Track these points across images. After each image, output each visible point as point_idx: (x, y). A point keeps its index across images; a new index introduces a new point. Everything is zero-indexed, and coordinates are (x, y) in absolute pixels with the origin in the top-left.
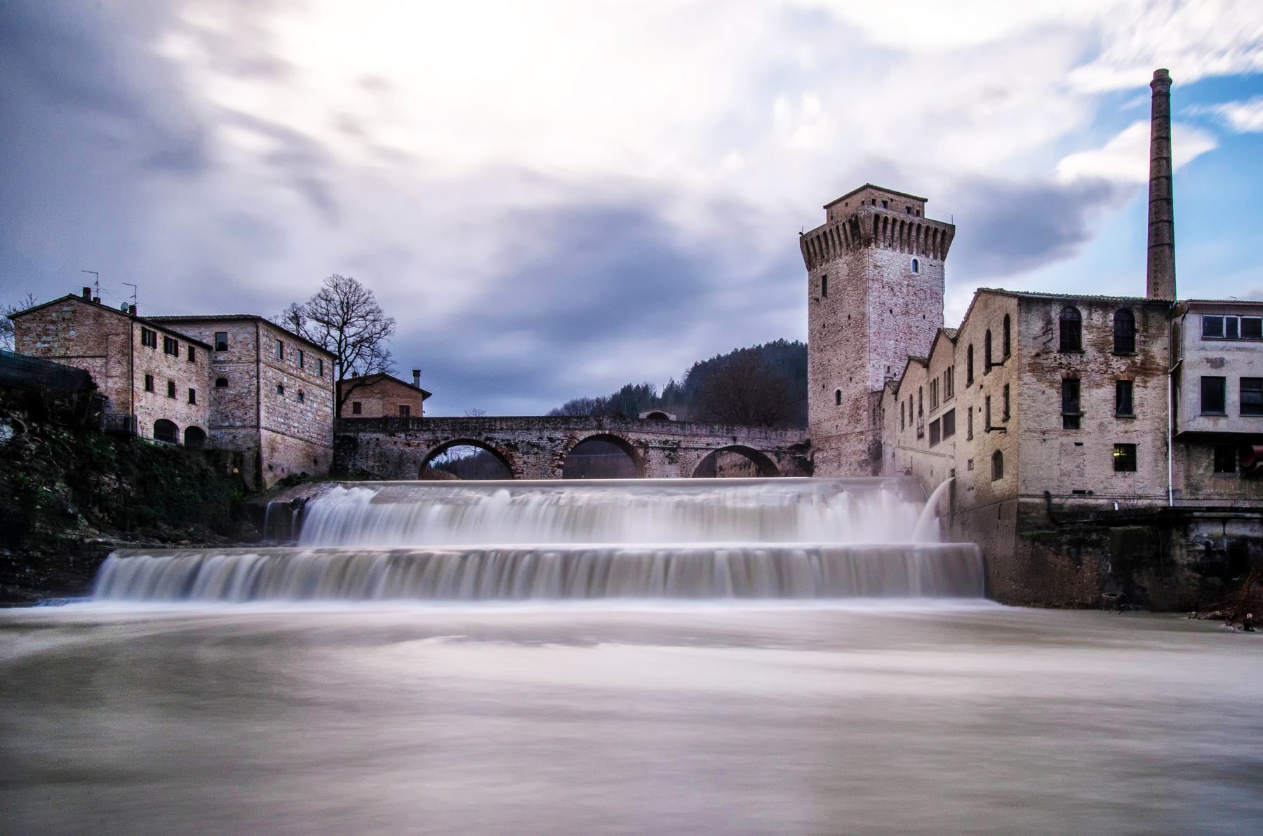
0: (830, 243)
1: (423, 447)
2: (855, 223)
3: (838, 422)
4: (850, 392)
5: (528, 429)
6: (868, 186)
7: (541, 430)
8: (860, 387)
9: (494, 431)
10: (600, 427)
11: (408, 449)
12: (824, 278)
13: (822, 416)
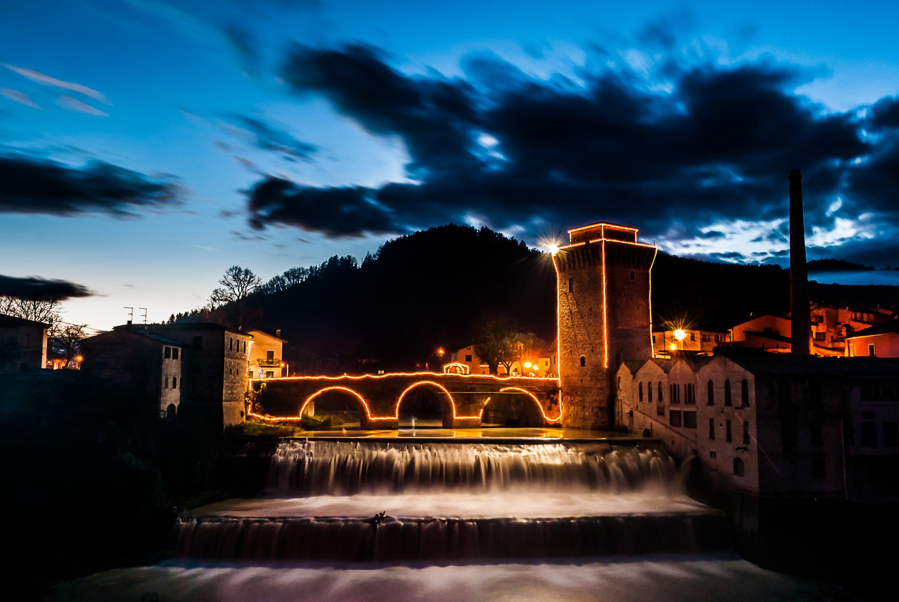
3: (583, 378)
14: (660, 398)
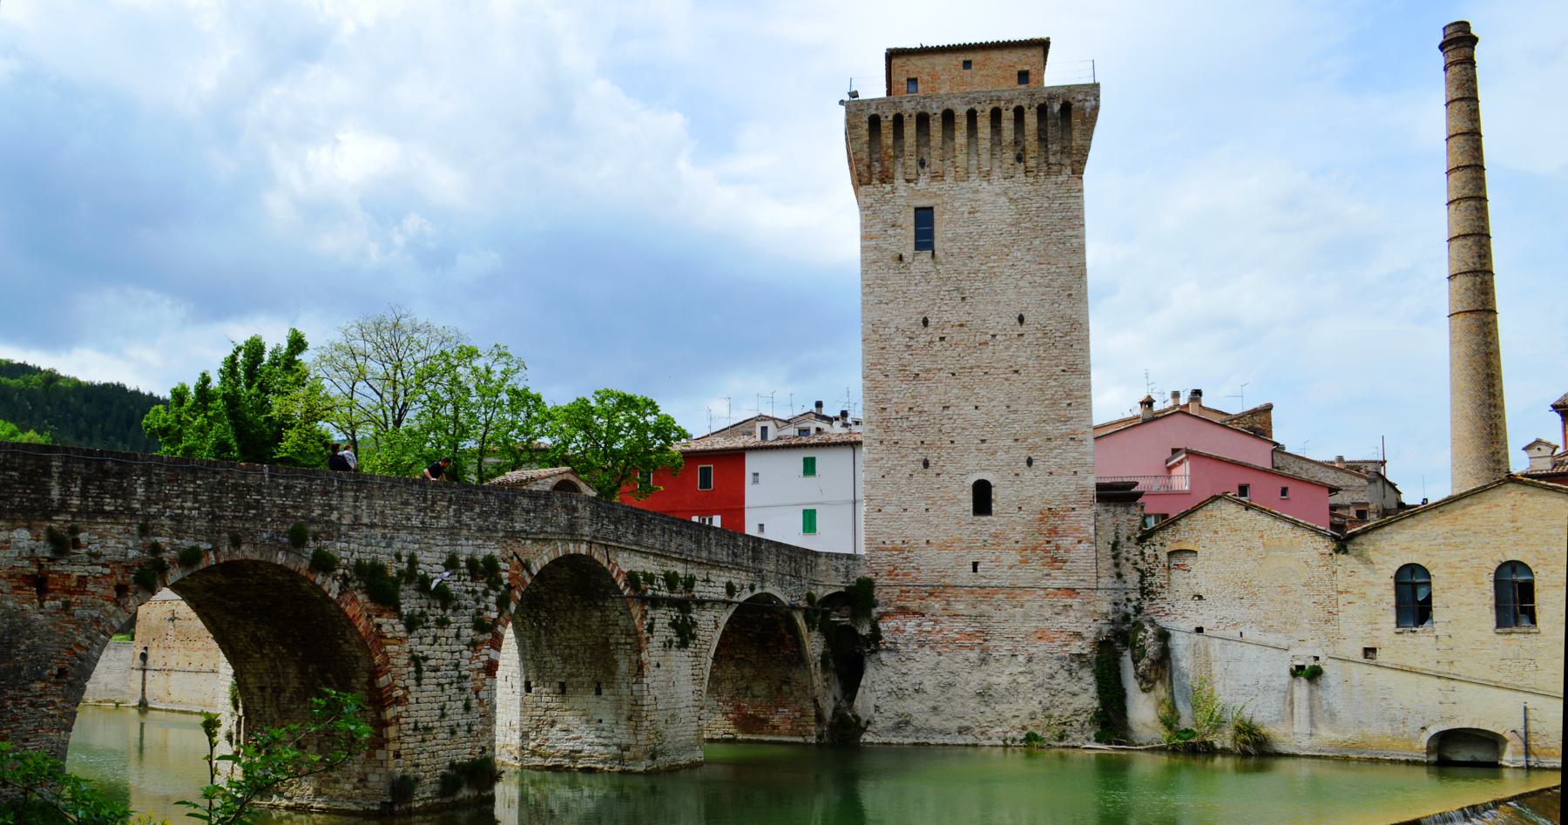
0: (961, 137)
5: (424, 528)
7: (452, 533)
9: (332, 530)
10: (571, 532)
12: (924, 218)
13: (918, 533)
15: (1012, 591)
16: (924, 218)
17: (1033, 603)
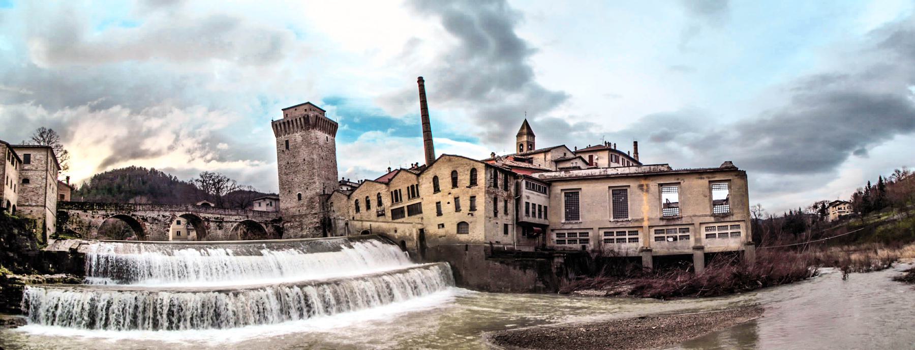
1: (101, 218)
2: (307, 118)
4: (307, 194)
6: (308, 103)
8: (313, 192)
10: (187, 210)
11: (93, 220)
12: (287, 142)
13: (289, 205)
14: (380, 203)
15: (306, 215)
16: (287, 142)
17: (309, 216)
